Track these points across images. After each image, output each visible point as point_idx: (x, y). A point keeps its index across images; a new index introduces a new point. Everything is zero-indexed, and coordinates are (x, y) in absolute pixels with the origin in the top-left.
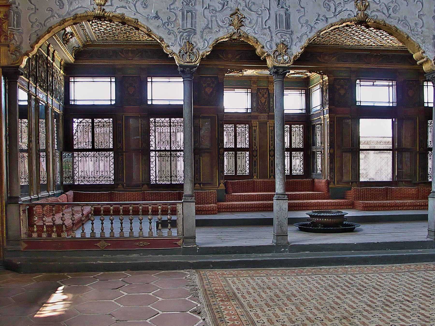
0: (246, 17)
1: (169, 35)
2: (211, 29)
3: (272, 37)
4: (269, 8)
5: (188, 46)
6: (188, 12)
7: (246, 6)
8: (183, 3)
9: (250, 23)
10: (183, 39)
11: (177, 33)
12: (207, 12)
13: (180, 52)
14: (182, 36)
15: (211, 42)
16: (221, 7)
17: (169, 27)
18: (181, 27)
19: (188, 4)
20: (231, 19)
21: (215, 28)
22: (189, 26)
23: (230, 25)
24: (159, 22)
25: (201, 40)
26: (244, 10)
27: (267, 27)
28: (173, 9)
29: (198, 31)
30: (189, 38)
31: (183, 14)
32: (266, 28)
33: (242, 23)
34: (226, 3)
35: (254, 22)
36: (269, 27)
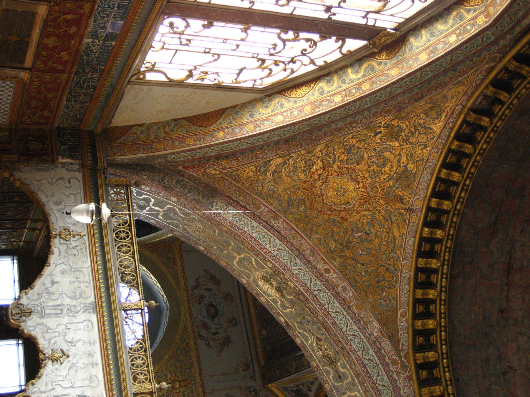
0: (63, 364)
1: (38, 294)
2: (47, 332)
3: (44, 392)
4: (74, 386)
5: (27, 311)
6: (61, 310)
7: (73, 364)
8: (69, 305)
9: (57, 369)
10: (34, 307)
11: (40, 301)
12: (63, 327)
13: (21, 304)
14: (38, 306)
15: (33, 333)
16: (70, 340)
17: (45, 294)
18: (46, 304)
19: (68, 309)
20: (59, 350)
21: (48, 336)
22: (47, 312)
23: (52, 350)
24: (48, 285)
25: (34, 324)
26: (69, 362)
27: (54, 387)
28: (62, 297)
29: (44, 321)
30: (35, 312)
31: (59, 306)
32: (53, 385)
33: (55, 362)
34: (73, 344)
35: (58, 373)
36: (54, 389)
